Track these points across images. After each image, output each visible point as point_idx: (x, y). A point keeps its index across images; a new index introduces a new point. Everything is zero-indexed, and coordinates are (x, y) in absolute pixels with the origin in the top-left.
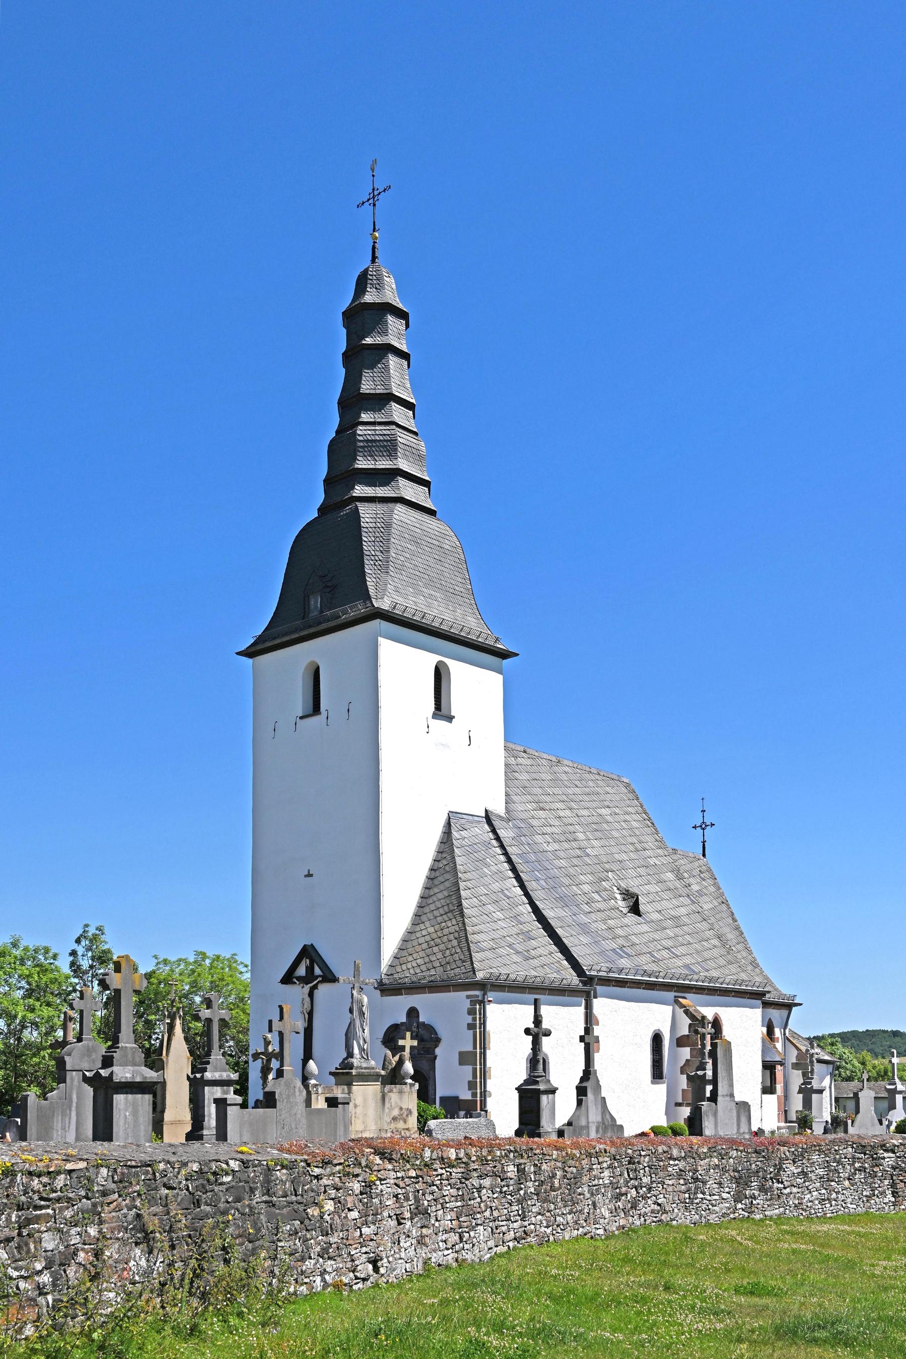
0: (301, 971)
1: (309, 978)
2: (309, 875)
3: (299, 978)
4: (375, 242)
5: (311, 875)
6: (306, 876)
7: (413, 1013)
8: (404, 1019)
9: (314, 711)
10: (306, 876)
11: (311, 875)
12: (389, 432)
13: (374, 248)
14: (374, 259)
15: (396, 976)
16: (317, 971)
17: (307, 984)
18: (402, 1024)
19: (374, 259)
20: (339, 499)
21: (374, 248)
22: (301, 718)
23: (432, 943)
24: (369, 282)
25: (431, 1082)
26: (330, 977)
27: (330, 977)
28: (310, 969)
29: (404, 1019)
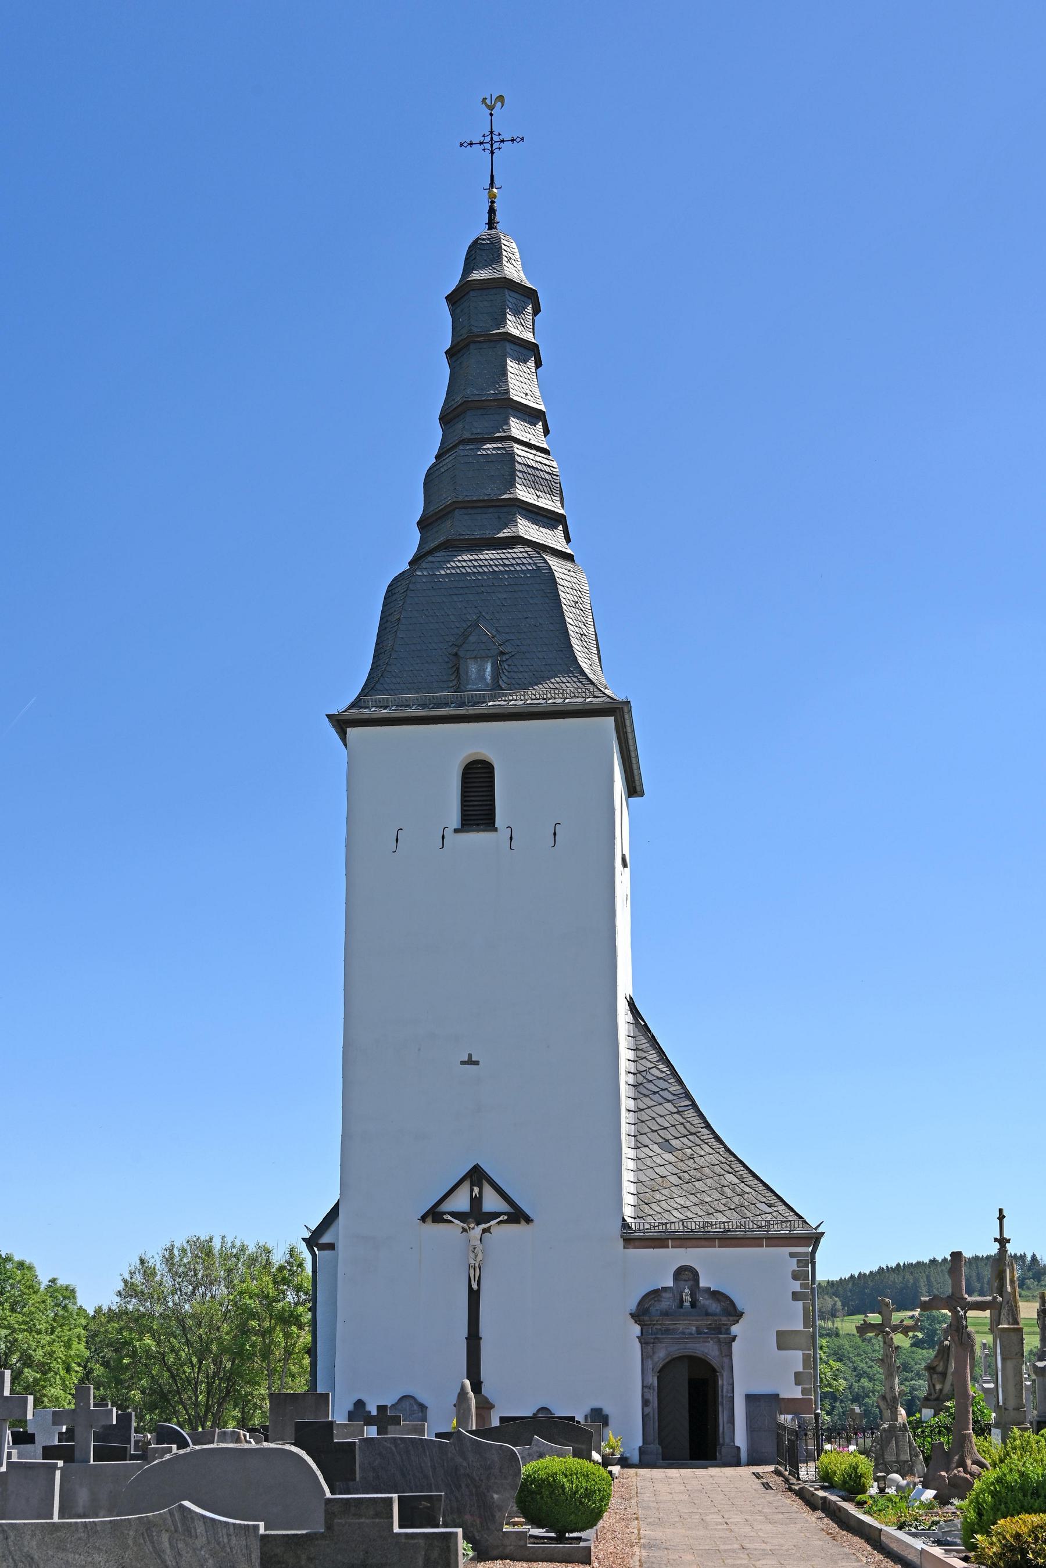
0: (461, 1202)
1: (476, 1214)
2: (470, 1062)
3: (456, 1215)
4: (493, 202)
5: (477, 1063)
6: (463, 1063)
7: (686, 1274)
8: (670, 1283)
9: (462, 825)
10: (463, 1063)
11: (477, 1063)
12: (547, 462)
13: (492, 211)
14: (491, 224)
15: (649, 1219)
16: (492, 1202)
17: (478, 1224)
18: (665, 1289)
19: (491, 224)
20: (488, 534)
21: (492, 211)
22: (456, 831)
23: (686, 1176)
24: (504, 253)
25: (725, 1374)
26: (517, 1216)
27: (517, 1216)
28: (476, 1202)
29: (670, 1283)
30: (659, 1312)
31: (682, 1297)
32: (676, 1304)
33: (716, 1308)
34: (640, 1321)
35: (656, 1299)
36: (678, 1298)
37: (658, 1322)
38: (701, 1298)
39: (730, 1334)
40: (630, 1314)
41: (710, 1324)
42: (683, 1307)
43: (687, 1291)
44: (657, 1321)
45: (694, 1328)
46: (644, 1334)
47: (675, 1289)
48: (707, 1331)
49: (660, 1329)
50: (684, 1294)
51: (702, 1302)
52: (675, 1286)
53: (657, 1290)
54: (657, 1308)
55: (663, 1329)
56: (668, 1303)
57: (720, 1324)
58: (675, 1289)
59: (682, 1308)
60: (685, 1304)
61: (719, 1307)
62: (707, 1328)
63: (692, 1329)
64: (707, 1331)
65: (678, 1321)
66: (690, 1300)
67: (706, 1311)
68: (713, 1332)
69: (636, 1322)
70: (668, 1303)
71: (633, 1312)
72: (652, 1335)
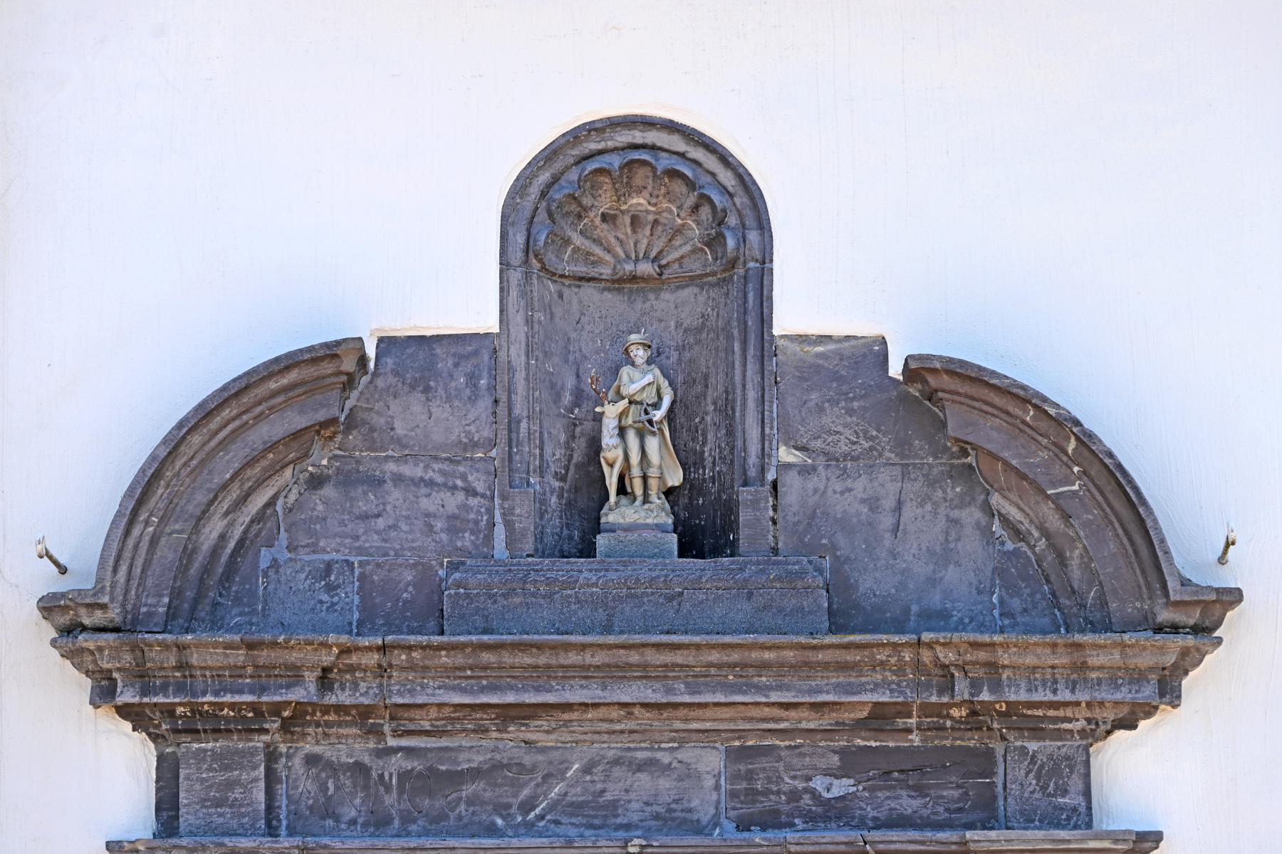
30: (350, 595)
31: (595, 446)
32: (524, 510)
33: (944, 556)
34: (142, 677)
35: (321, 458)
36: (555, 454)
37: (344, 697)
38: (786, 455)
39: (1082, 817)
40: (49, 606)
41: (880, 718)
42: (601, 541)
43: (636, 381)
44: (325, 679)
45: (711, 761)
46: (186, 818)
47: (516, 354)
48: (841, 787)
49: (360, 769)
50: (611, 412)
51: (793, 488)
52: (519, 330)
53: (331, 351)
54: (332, 551)
55: (398, 763)
56: (453, 502)
57: (976, 716)
58: (516, 354)
59: (587, 550)
60: (618, 514)
61: (971, 544)
62: (850, 763)
63: (689, 774)
64: (841, 787)
65: (542, 676)
66: (675, 478)
67: (838, 586)
68: (908, 804)
69: (104, 693)
70: (453, 502)
71: (83, 578)
72: (272, 831)
